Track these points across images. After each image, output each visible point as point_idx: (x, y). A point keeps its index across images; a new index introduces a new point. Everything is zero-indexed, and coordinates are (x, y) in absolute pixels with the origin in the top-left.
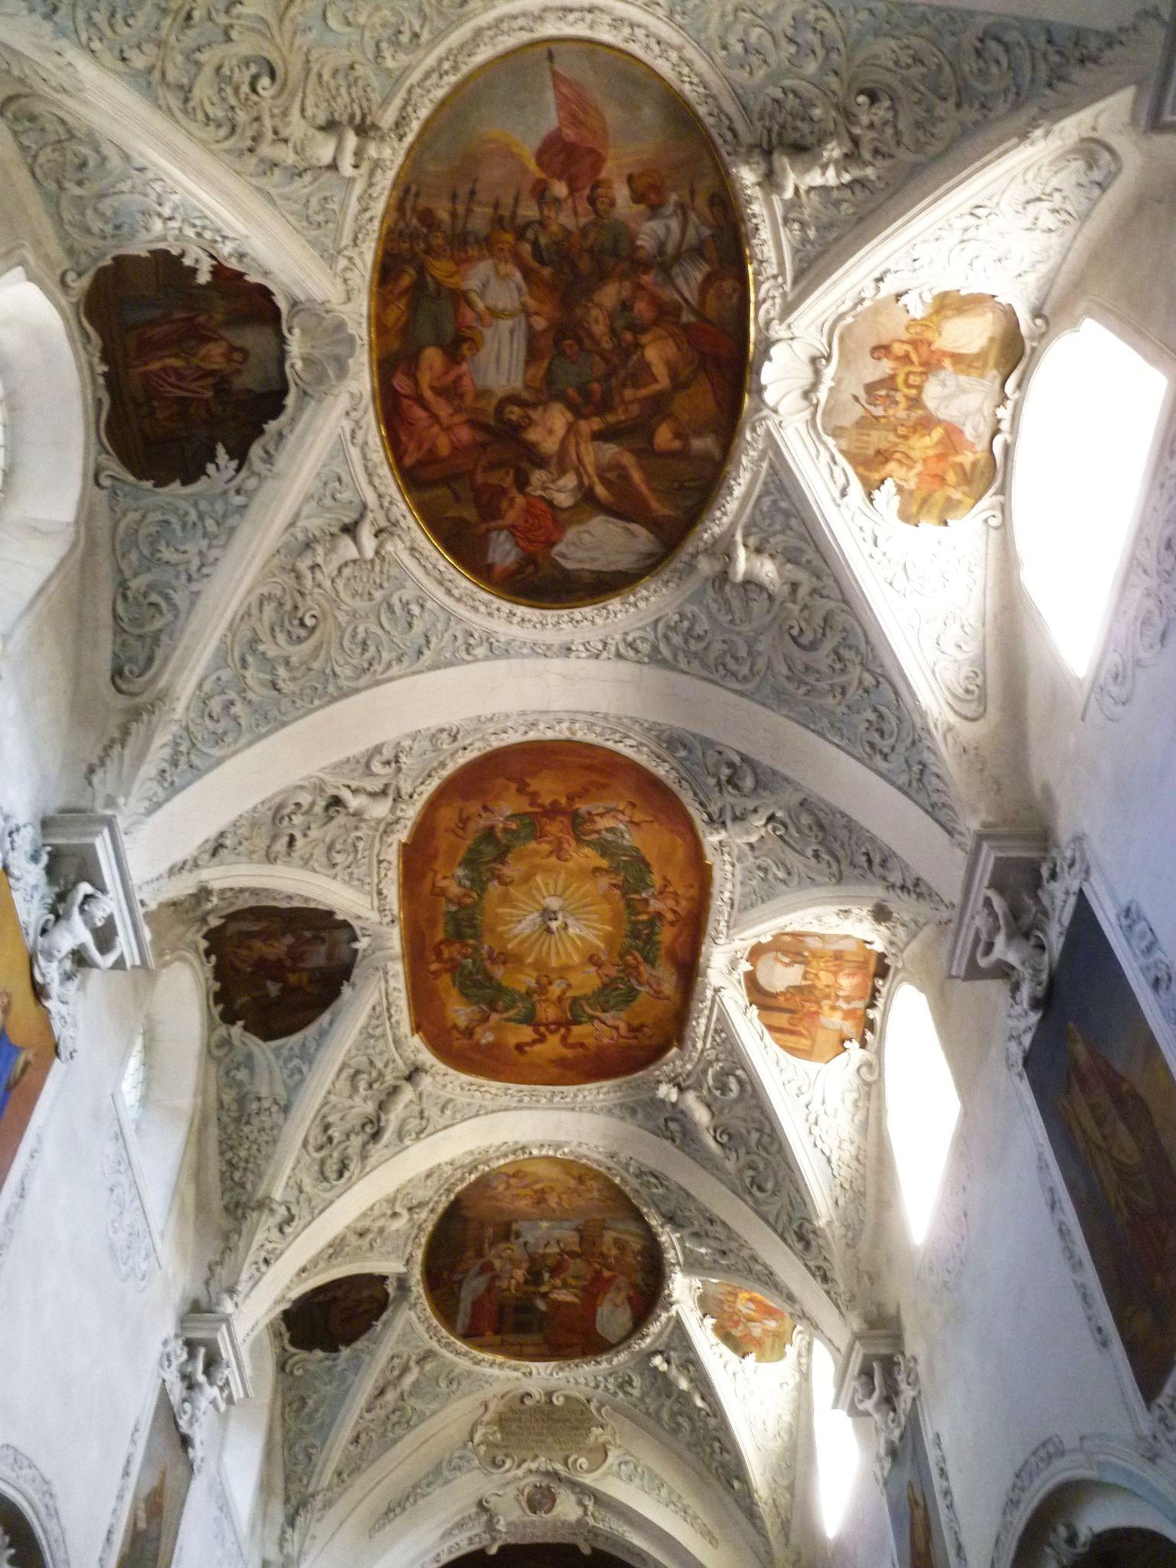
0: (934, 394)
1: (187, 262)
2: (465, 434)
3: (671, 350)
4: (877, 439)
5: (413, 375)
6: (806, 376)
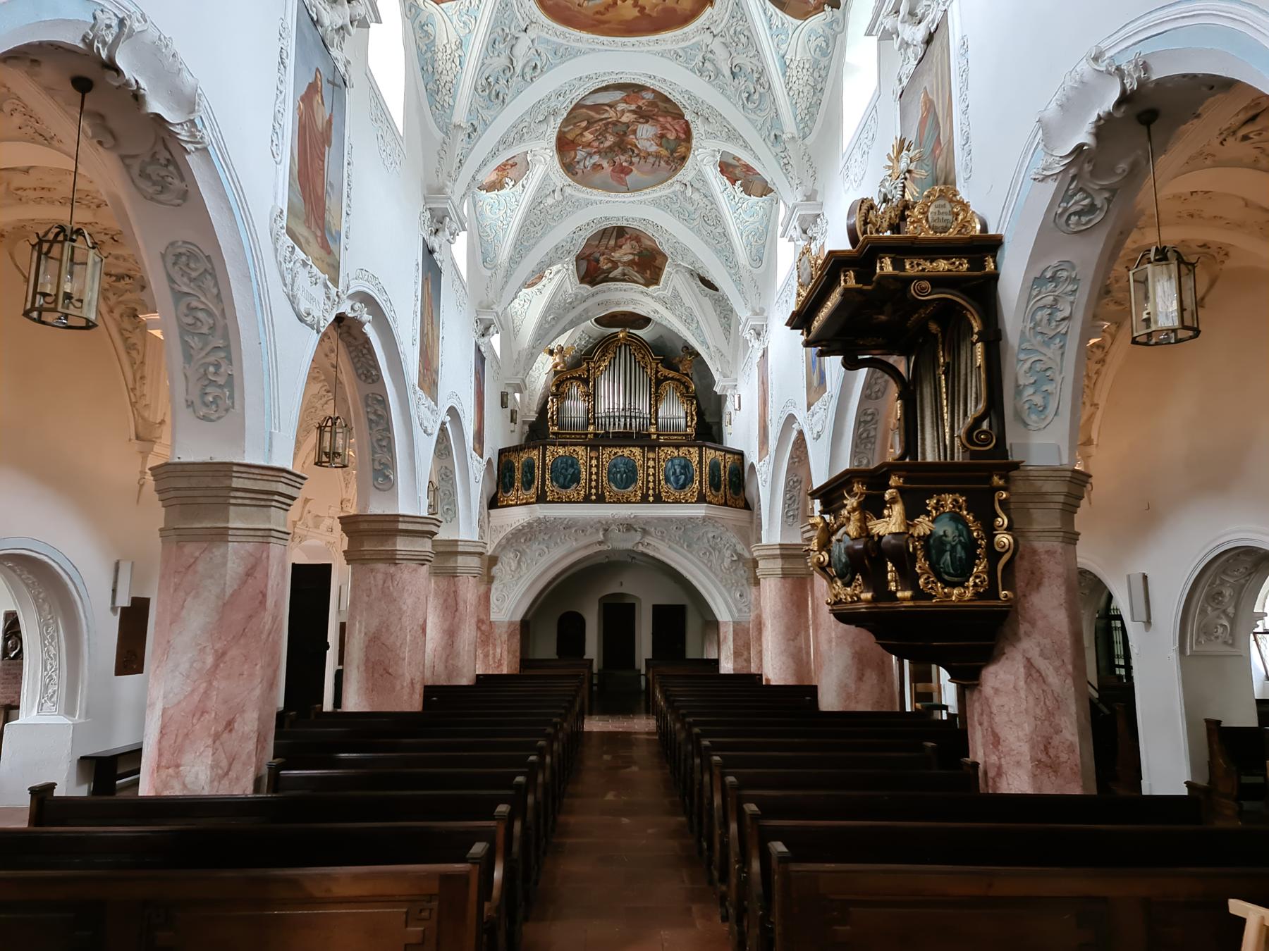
2: (661, 119)
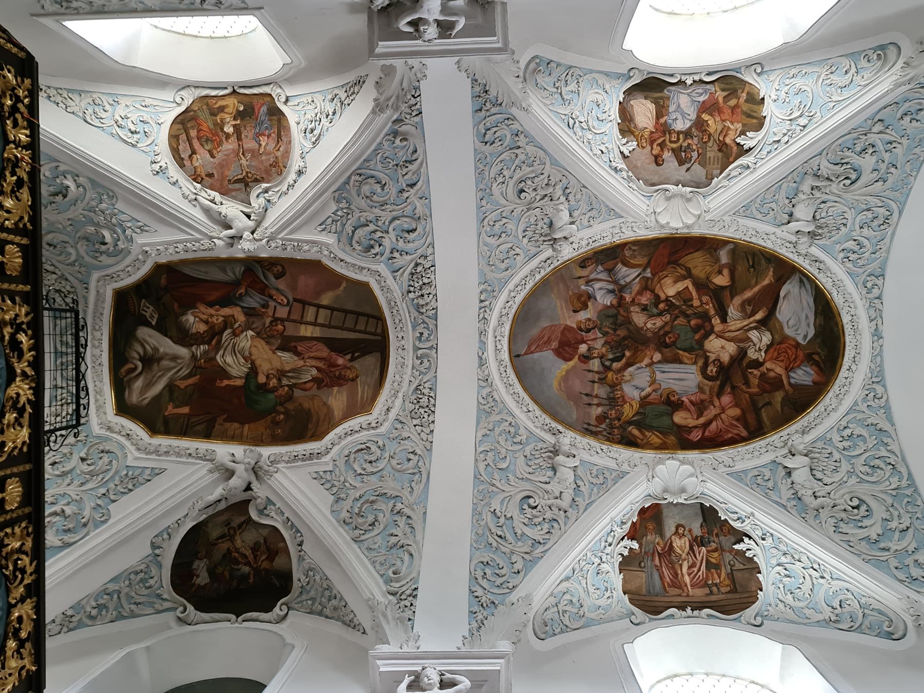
0: (681, 125)
1: (626, 553)
2: (726, 399)
3: (668, 281)
4: (712, 152)
5: (690, 430)
6: (677, 203)
